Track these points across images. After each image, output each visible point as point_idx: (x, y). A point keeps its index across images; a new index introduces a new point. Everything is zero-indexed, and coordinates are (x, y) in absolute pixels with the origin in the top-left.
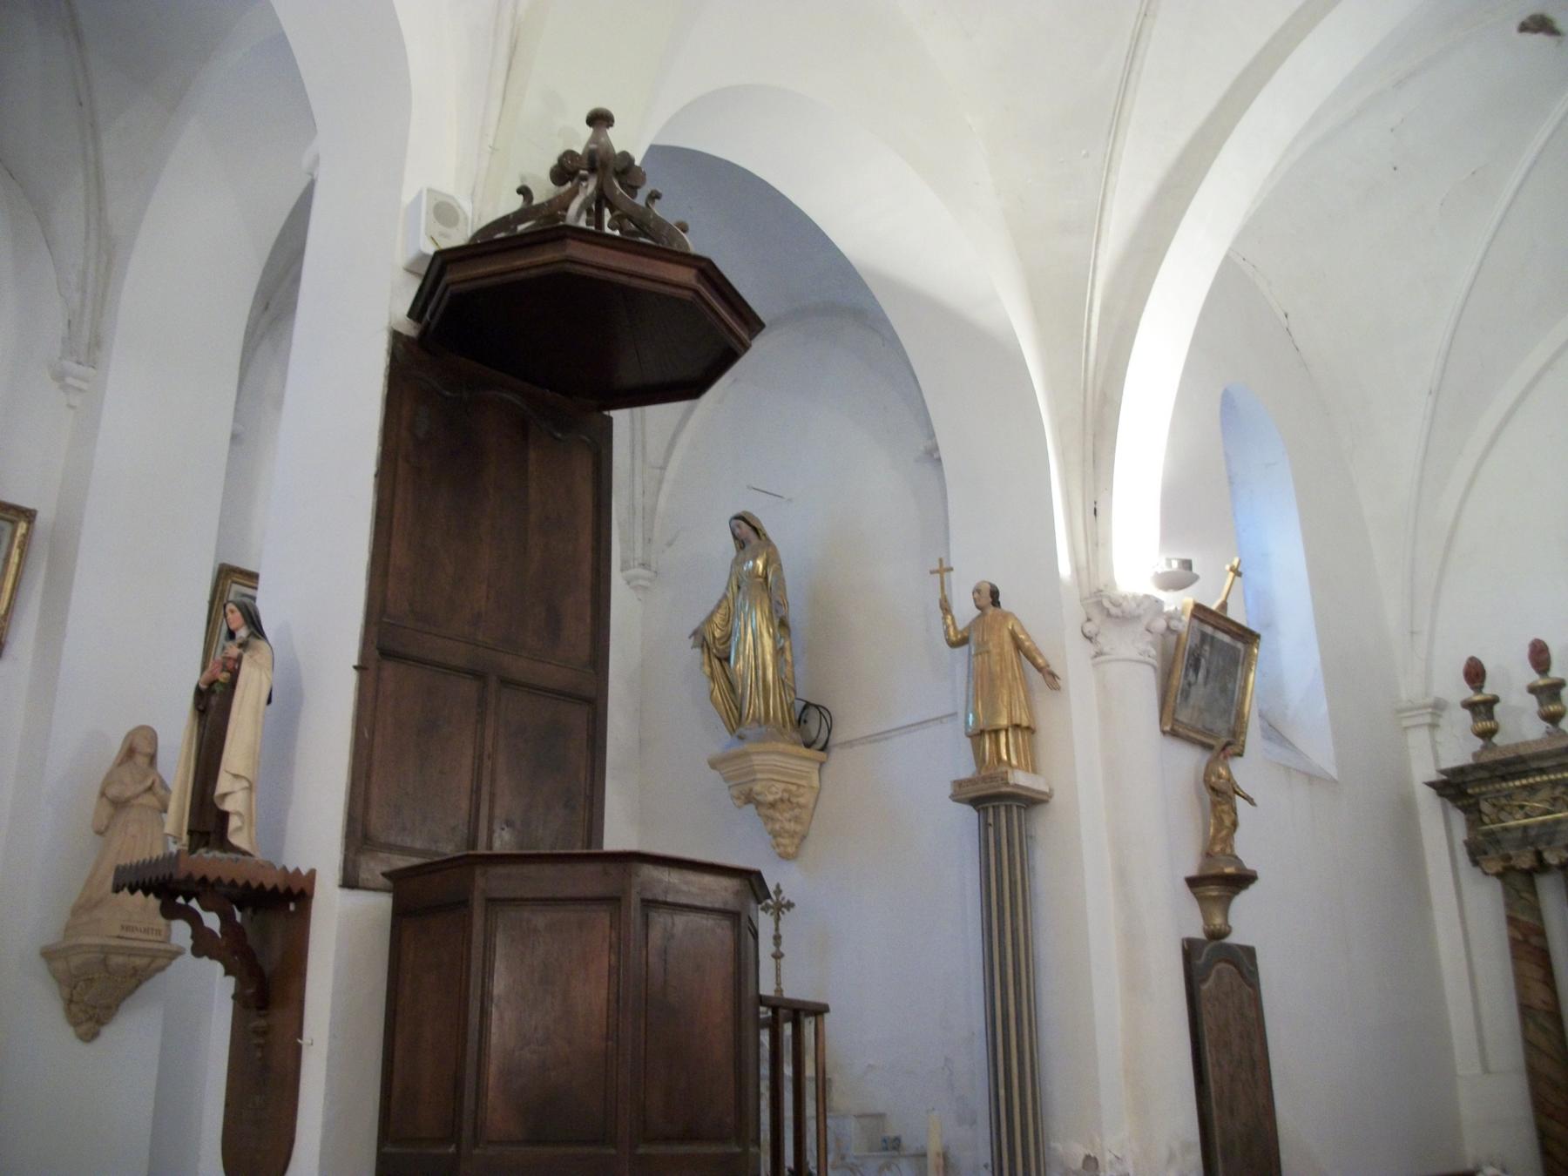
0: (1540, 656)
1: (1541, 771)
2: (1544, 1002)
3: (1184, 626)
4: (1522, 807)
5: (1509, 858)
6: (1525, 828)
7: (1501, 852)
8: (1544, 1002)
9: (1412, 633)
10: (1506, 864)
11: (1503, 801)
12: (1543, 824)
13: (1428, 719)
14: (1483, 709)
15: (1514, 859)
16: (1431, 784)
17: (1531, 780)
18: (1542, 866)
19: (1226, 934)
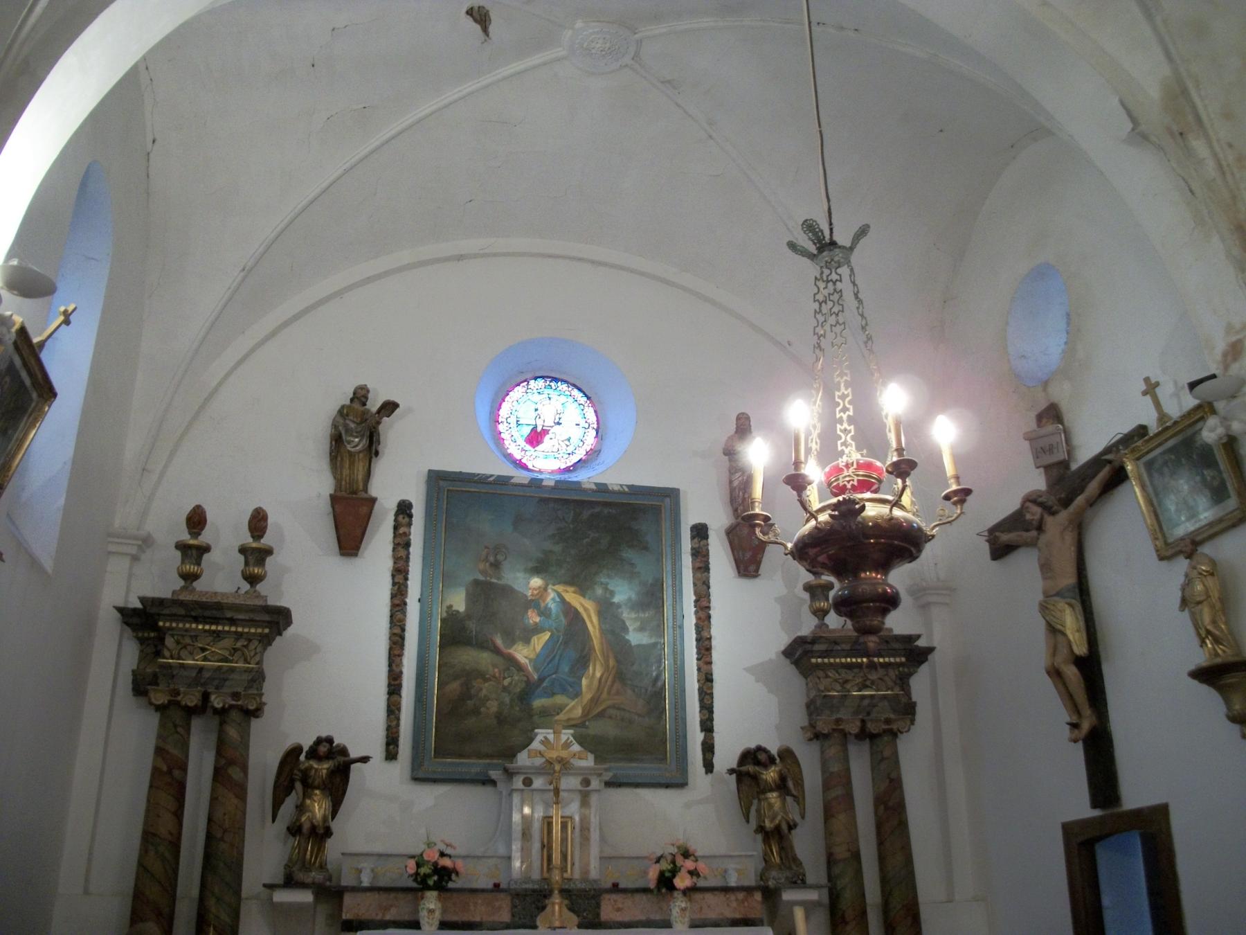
0: (258, 523)
1: (232, 622)
2: (171, 834)
3: (10, 339)
5: (178, 694)
6: (201, 669)
7: (172, 686)
8: (171, 834)
9: (144, 470)
11: (188, 640)
12: (220, 668)
13: (134, 551)
14: (193, 552)
15: (182, 696)
16: (121, 610)
17: (220, 628)
18: (203, 706)
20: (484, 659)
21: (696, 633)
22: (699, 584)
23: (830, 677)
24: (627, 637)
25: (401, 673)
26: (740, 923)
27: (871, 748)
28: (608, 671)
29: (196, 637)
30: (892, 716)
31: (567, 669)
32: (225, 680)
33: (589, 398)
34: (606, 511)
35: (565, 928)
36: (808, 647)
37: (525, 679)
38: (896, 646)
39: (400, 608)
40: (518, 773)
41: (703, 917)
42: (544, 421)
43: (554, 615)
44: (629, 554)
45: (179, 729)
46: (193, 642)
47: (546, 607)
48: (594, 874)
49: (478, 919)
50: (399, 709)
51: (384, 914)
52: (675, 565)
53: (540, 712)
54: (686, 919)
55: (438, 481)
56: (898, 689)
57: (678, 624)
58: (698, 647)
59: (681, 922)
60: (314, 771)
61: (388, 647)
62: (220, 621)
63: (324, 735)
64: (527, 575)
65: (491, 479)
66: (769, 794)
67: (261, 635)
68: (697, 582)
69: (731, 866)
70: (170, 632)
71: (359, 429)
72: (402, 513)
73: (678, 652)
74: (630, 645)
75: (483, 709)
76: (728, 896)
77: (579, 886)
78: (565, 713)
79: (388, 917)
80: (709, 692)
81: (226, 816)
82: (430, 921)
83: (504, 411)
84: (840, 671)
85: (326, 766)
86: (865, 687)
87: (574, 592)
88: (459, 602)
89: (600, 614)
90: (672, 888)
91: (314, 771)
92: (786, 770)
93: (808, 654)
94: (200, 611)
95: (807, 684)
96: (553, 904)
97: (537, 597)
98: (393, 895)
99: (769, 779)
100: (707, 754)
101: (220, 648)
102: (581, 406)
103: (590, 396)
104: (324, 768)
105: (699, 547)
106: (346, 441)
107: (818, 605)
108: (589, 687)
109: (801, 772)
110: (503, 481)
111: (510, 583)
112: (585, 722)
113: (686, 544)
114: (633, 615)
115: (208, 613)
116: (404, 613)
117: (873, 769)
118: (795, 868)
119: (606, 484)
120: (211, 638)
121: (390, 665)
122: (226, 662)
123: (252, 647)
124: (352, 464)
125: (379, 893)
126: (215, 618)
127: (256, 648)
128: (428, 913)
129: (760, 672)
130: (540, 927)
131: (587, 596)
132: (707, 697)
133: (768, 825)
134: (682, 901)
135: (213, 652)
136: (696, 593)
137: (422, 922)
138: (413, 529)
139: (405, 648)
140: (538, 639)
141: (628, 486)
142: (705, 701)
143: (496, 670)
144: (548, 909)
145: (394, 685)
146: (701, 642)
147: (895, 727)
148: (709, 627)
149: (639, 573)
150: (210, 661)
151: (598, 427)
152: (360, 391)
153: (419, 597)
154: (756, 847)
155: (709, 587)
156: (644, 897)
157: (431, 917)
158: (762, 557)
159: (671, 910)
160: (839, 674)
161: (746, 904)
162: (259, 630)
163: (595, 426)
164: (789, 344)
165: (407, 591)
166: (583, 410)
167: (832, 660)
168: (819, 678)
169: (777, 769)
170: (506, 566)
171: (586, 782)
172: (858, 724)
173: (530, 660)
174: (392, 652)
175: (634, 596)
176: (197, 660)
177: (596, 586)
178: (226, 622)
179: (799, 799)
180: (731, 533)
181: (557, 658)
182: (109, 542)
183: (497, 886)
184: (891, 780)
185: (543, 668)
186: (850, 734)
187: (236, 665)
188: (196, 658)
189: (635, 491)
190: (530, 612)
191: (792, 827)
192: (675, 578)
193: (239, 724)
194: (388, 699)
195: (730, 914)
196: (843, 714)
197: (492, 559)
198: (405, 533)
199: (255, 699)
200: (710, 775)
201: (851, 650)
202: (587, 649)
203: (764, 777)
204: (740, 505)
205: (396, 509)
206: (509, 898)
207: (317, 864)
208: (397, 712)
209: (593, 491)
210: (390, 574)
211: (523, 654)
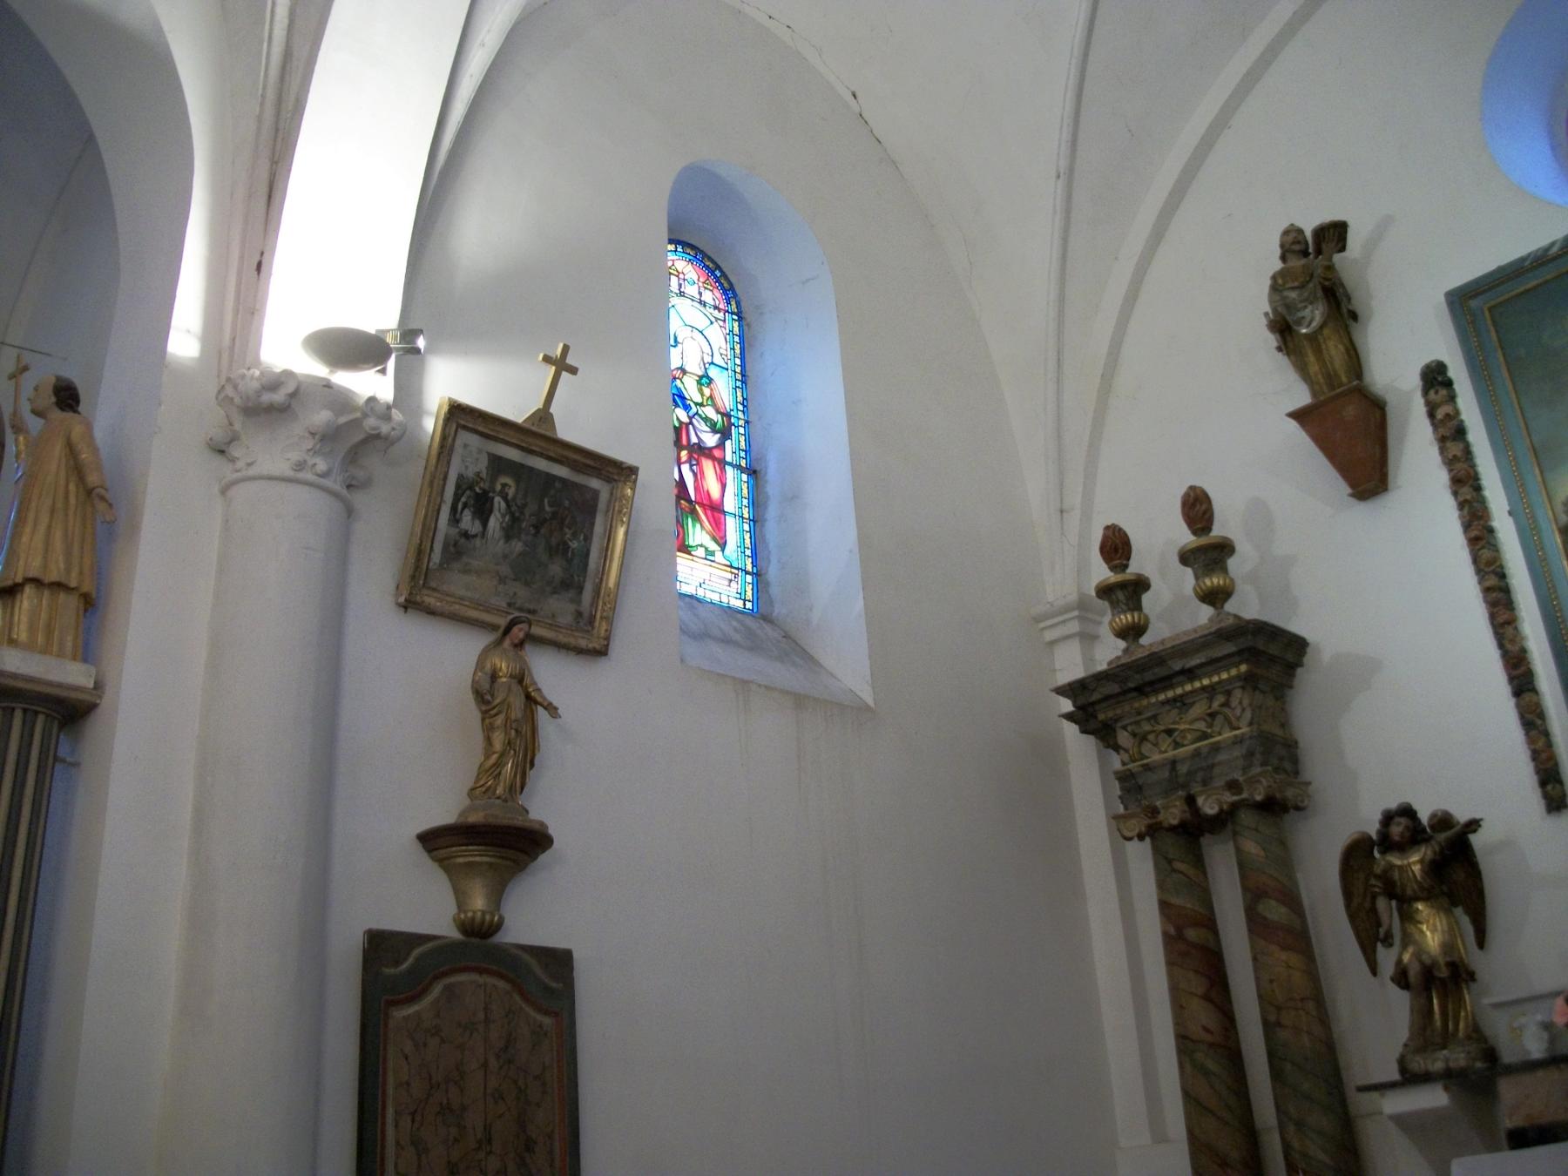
0: (1197, 508)
1: (1190, 674)
4: (1169, 732)
5: (1154, 811)
6: (1173, 763)
7: (1145, 802)
9: (1062, 512)
10: (1150, 821)
11: (1147, 727)
13: (1074, 627)
15: (1162, 811)
19: (497, 927)
25: (1524, 651)
29: (1155, 717)
32: (1212, 766)
39: (1484, 541)
45: (1178, 865)
55: (1462, 301)
61: (1487, 615)
62: (1174, 681)
63: (1393, 805)
65: (1555, 249)
67: (1239, 677)
70: (1119, 724)
71: (1306, 294)
81: (1275, 984)
85: (1415, 858)
94: (1137, 676)
101: (1191, 720)
104: (1414, 862)
115: (1149, 676)
120: (1175, 711)
121: (1501, 646)
123: (1234, 702)
124: (1318, 351)
127: (1240, 703)
135: (1182, 731)
139: (1515, 605)
150: (1183, 746)
162: (1234, 672)
176: (1166, 752)
178: (1181, 678)
182: (1043, 629)
188: (1163, 749)
193: (1256, 830)
194: (1518, 706)
198: (1447, 415)
199: (1259, 781)
207: (1461, 1034)
208: (1539, 722)
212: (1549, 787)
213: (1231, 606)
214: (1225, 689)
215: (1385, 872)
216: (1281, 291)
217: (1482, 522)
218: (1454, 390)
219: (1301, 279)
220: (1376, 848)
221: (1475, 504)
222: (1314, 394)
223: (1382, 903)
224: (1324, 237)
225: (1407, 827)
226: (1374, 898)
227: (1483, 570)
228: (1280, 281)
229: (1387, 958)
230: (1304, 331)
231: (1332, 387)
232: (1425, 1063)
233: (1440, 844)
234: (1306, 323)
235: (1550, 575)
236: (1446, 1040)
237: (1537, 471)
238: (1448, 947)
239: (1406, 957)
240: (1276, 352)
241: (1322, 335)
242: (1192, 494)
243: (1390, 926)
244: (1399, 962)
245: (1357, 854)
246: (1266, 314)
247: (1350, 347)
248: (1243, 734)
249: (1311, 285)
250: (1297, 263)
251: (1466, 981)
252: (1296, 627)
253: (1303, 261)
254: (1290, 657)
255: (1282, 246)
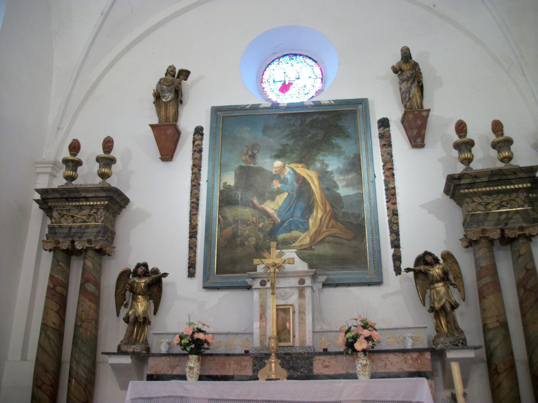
0: (108, 144)
1: (87, 199)
2: (54, 323)
4: (73, 217)
5: (58, 243)
6: (71, 228)
7: (56, 239)
8: (54, 323)
9: (58, 129)
10: (55, 246)
11: (65, 212)
13: (49, 170)
15: (61, 244)
20: (245, 212)
21: (385, 186)
22: (385, 155)
23: (475, 202)
24: (338, 191)
25: (197, 225)
26: (415, 375)
27: (511, 248)
28: (326, 212)
29: (69, 210)
30: (524, 225)
31: (299, 215)
32: (84, 233)
33: (316, 62)
34: (321, 117)
35: (279, 379)
36: (457, 182)
37: (273, 222)
38: (522, 175)
39: (196, 187)
40: (257, 278)
41: (387, 371)
42: (290, 78)
43: (290, 183)
44: (337, 141)
45: (61, 264)
46: (67, 213)
47: (284, 178)
48: (309, 342)
49: (232, 374)
50: (196, 246)
51: (172, 371)
52: (367, 144)
53: (282, 242)
54: (367, 373)
55: (216, 111)
56: (527, 206)
57: (371, 180)
58: (386, 194)
59: (363, 374)
60: (136, 284)
61: (190, 210)
63: (141, 262)
64: (272, 160)
65: (248, 107)
66: (436, 284)
68: (384, 154)
69: (408, 334)
70: (55, 209)
71: (169, 89)
72: (197, 133)
73: (372, 198)
74: (340, 196)
75: (246, 243)
76: (405, 356)
77: (298, 351)
78: (298, 242)
79: (175, 373)
80: (395, 222)
81: (83, 312)
82: (191, 375)
83: (265, 77)
84: (482, 197)
85: (143, 281)
86: (502, 206)
87: (302, 167)
88: (230, 179)
89: (320, 179)
90: (354, 351)
91: (136, 284)
92: (448, 268)
93: (457, 187)
94: (68, 194)
95: (462, 211)
96: (271, 363)
97: (279, 172)
98: (178, 358)
99: (435, 274)
100: (396, 262)
101: (82, 215)
102: (311, 67)
103: (316, 60)
104: (142, 282)
105: (384, 133)
106: (162, 96)
107: (463, 156)
108: (314, 224)
109: (459, 268)
110: (255, 107)
111: (261, 166)
112: (312, 246)
113: (375, 131)
114: (341, 178)
115: (72, 195)
116: (199, 190)
117: (514, 263)
118: (457, 335)
119: (319, 101)
121: (190, 221)
122: (85, 223)
123: (99, 213)
124: (166, 109)
125: (169, 358)
126: (76, 198)
127: (101, 214)
128: (189, 369)
129: (431, 207)
130: (260, 379)
131: (310, 169)
132: (395, 225)
133: (437, 306)
134: (363, 360)
136: (383, 161)
137: (187, 376)
138: (204, 141)
139: (199, 210)
140: (280, 197)
141: (333, 101)
142: (393, 228)
143: (254, 218)
144: (267, 366)
145: (193, 232)
146: (388, 191)
147: (527, 232)
148: (394, 181)
149: (344, 151)
150: (76, 223)
151: (322, 77)
152: (169, 68)
153: (207, 179)
154: (429, 321)
155: (392, 156)
156: (344, 358)
157: (191, 372)
158: (425, 132)
159: (356, 366)
160: (482, 199)
161: (419, 361)
162: (102, 203)
163: (321, 77)
164: (434, 6)
165: (200, 177)
166: (312, 69)
167: (475, 190)
168: (467, 203)
169: (441, 267)
170: (259, 156)
171: (302, 282)
172: (499, 231)
173: (275, 211)
174: (191, 213)
175: (341, 166)
176: (69, 223)
177: (316, 162)
178: (83, 199)
179: (461, 289)
180: (404, 120)
181: (292, 208)
182: (37, 167)
183: (247, 352)
184: (528, 270)
185: (284, 215)
186: (495, 240)
187: (90, 224)
189: (339, 103)
190: (274, 182)
191: (454, 307)
192: (368, 152)
193: (93, 258)
194: (189, 241)
195: (406, 368)
196: (487, 226)
197: (250, 153)
198: (199, 144)
199: (99, 242)
200: (399, 276)
201: (489, 181)
202: (312, 200)
203: (431, 272)
204: (407, 102)
205: (194, 131)
206: (251, 360)
207: (141, 341)
208: (194, 248)
209: (312, 106)
210: (191, 168)
211: (271, 207)
212: (191, 269)
213: (108, 181)
214: (97, 207)
215: (132, 283)
216: (162, 85)
217: (197, 181)
218: (203, 137)
219: (169, 84)
220: (131, 274)
221: (197, 175)
222: (159, 122)
223: (128, 293)
224: (182, 73)
225: (144, 270)
226: (126, 290)
227: (192, 196)
228: (162, 81)
229: (124, 312)
230: (164, 100)
231: (166, 121)
232: (127, 348)
233: (152, 278)
234: (165, 98)
235: (212, 204)
236: (136, 342)
237: (219, 171)
238: (145, 312)
239: (130, 313)
240: (153, 103)
241: (169, 104)
242: (108, 139)
243: (128, 301)
244: (128, 313)
245: (125, 275)
246: (154, 90)
247: (176, 112)
248: (99, 225)
249: (172, 87)
250: (170, 78)
251: (147, 325)
252: (128, 194)
253: (172, 78)
254: (122, 204)
255: (167, 71)
